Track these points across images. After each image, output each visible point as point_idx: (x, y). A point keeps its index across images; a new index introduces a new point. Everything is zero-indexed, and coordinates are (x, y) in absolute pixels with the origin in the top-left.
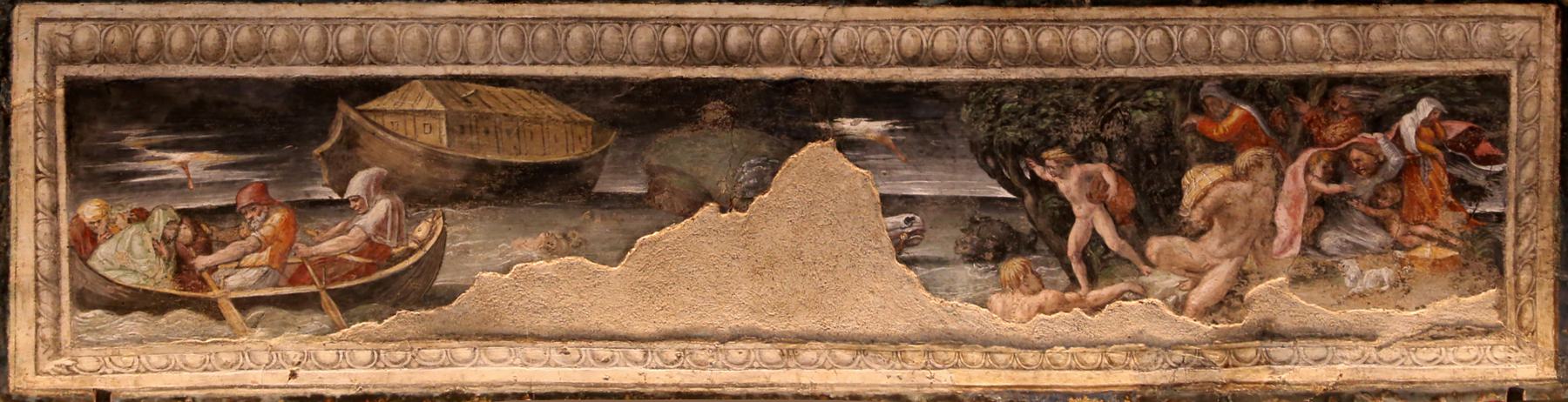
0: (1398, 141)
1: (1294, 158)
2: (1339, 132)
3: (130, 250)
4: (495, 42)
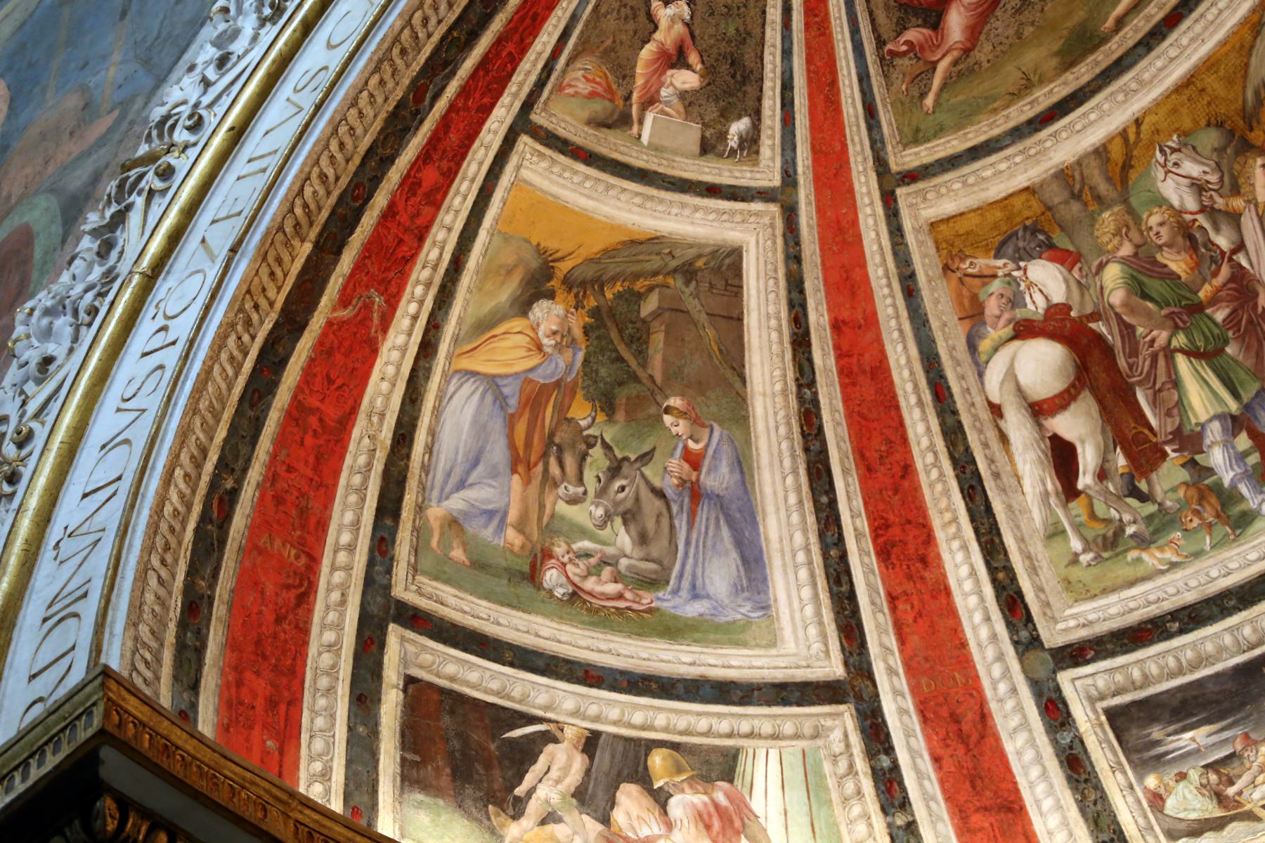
3: (1185, 798)
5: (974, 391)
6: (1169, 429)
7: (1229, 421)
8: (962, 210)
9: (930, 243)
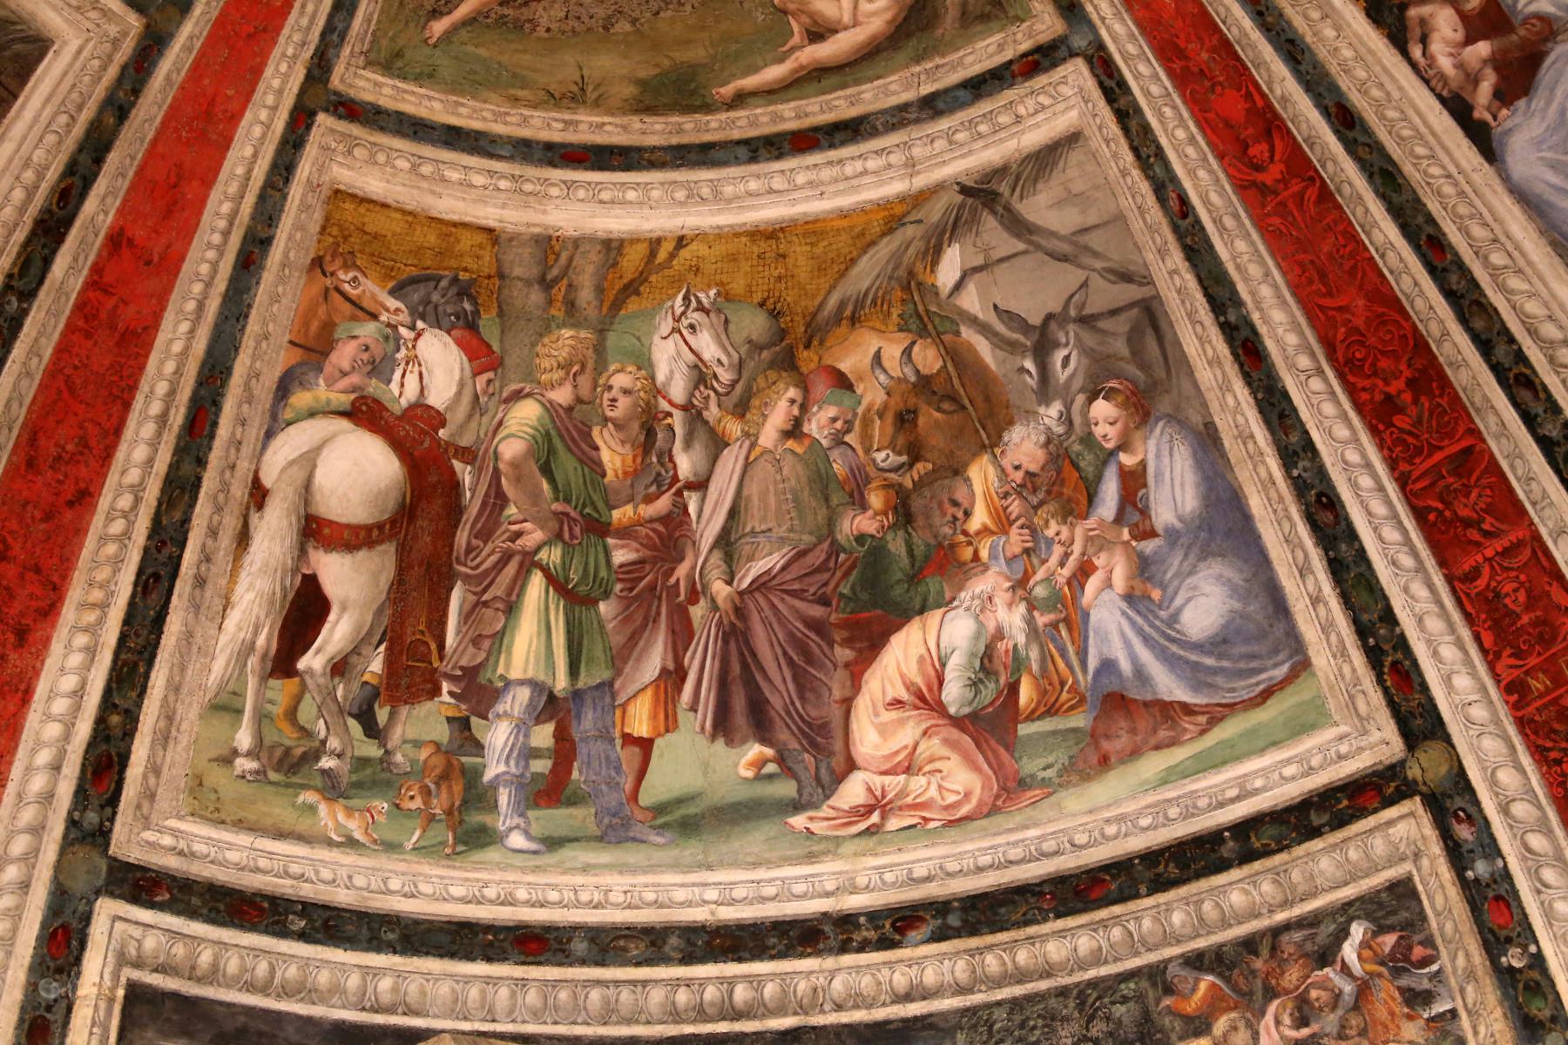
0: (1345, 970)
1: (1263, 1013)
2: (1294, 977)
4: (520, 1001)
5: (246, 450)
6: (464, 662)
7: (544, 698)
8: (389, 201)
9: (318, 216)
